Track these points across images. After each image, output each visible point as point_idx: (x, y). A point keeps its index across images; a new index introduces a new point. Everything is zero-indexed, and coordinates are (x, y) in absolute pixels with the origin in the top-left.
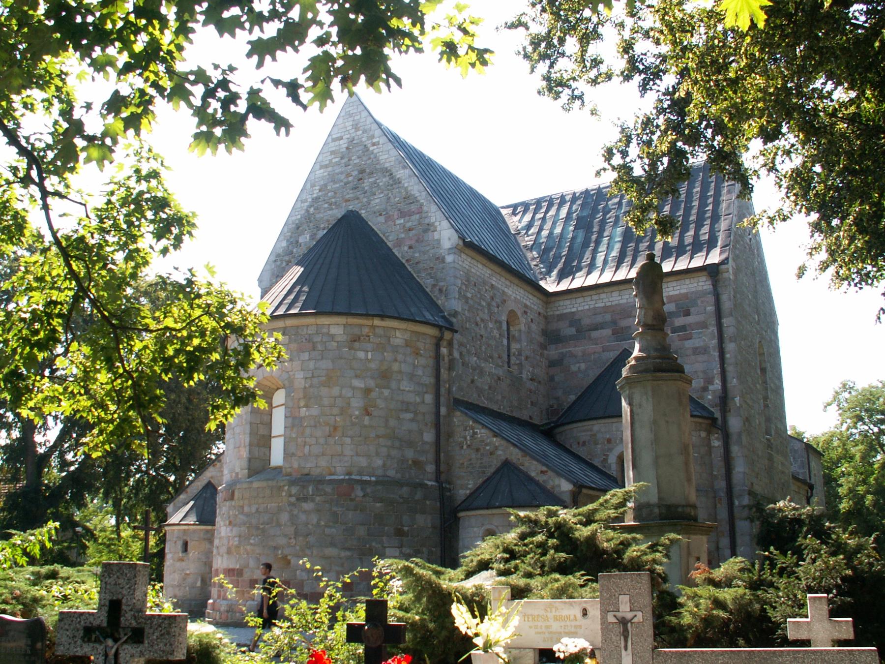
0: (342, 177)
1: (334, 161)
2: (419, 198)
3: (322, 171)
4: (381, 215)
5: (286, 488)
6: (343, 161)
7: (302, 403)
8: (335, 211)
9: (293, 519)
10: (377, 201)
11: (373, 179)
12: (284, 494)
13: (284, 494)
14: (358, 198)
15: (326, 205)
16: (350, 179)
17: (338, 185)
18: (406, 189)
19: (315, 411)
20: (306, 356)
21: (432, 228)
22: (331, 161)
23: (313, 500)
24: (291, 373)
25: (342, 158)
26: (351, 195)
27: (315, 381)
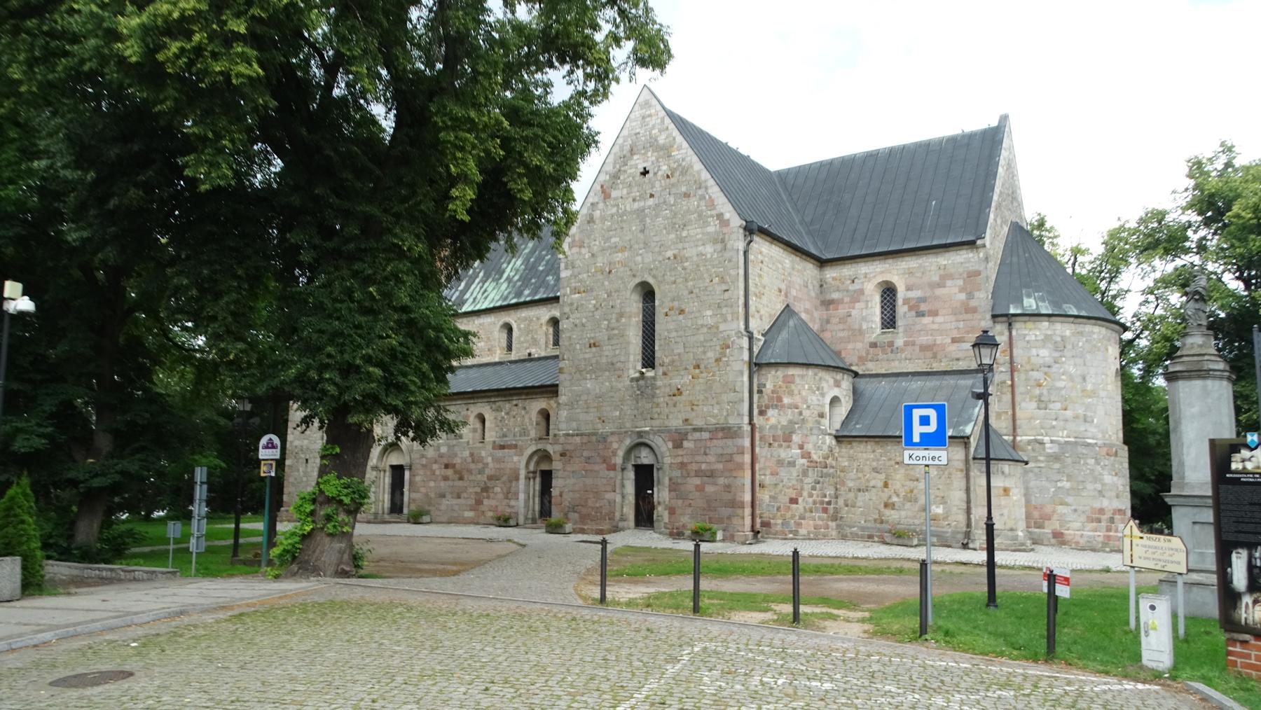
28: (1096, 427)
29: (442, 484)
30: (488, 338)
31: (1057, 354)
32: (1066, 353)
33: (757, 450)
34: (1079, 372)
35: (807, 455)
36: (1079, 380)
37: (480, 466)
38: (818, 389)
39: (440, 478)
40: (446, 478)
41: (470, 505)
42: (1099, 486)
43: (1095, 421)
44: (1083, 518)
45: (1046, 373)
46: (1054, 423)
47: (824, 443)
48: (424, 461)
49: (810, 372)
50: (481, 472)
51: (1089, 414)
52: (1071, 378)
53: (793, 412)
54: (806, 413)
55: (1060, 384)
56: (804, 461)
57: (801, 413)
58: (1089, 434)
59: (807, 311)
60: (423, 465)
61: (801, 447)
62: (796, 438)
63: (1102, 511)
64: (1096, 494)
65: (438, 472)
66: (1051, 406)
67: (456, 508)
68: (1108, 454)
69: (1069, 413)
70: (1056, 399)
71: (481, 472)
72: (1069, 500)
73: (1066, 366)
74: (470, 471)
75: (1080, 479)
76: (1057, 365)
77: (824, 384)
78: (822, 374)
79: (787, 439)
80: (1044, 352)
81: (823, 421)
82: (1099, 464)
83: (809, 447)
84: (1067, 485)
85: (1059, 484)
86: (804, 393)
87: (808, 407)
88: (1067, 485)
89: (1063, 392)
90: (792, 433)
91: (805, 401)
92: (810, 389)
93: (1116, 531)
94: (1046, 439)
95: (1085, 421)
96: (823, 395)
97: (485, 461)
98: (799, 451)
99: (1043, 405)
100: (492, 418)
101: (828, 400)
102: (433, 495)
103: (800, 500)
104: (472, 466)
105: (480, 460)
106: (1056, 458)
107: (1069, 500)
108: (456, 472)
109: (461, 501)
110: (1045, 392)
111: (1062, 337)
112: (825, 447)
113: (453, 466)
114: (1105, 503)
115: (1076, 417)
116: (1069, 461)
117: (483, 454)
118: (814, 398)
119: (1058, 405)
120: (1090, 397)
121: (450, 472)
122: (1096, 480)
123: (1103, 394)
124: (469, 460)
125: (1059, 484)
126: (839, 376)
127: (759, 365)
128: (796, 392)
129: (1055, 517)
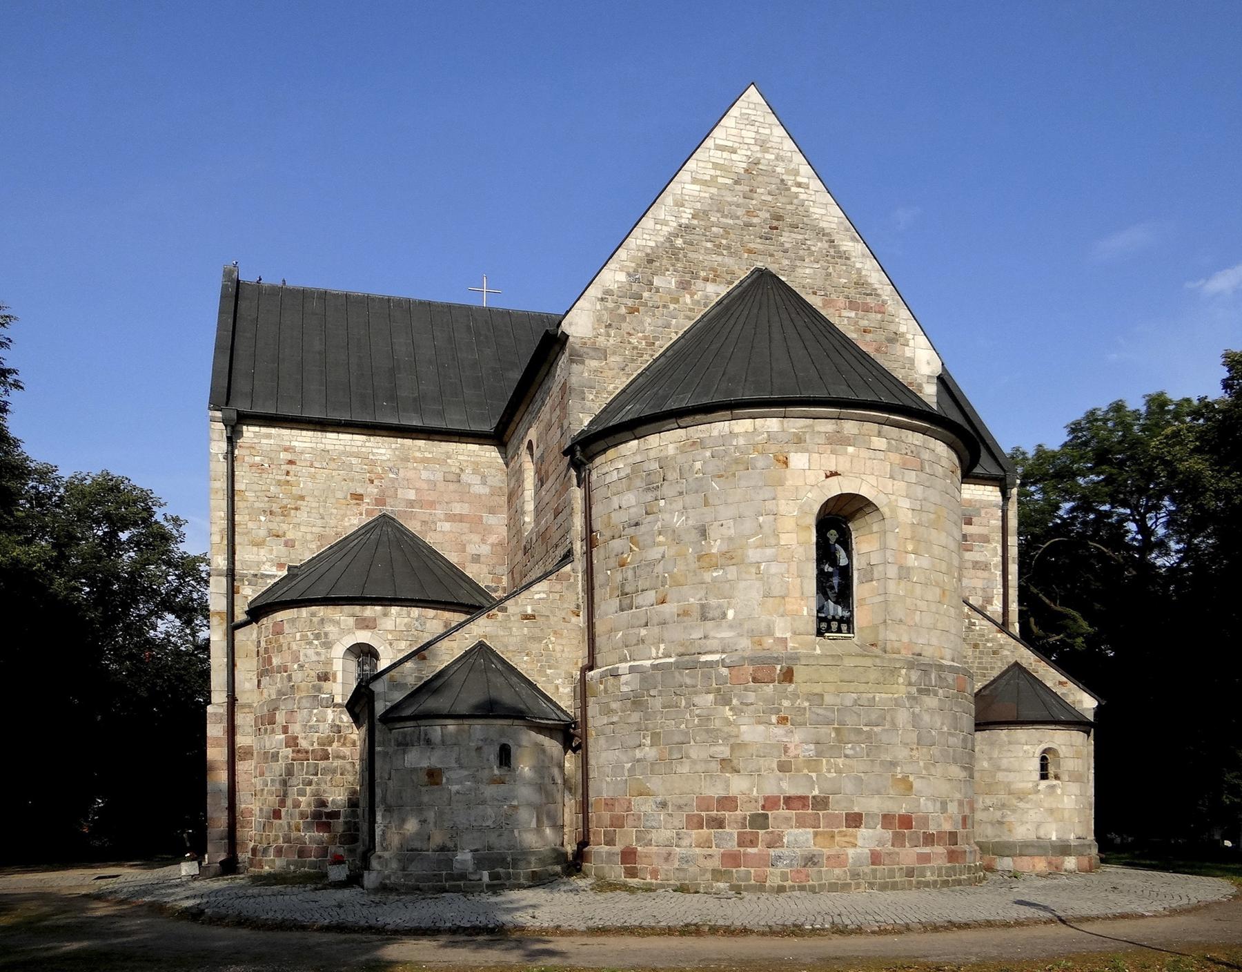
0: (740, 212)
1: (720, 180)
2: (879, 292)
3: (697, 187)
4: (815, 293)
5: (903, 671)
6: (738, 187)
7: (910, 548)
8: (730, 261)
9: (915, 719)
10: (807, 271)
11: (800, 237)
12: (901, 680)
13: (901, 680)
14: (771, 255)
15: (709, 245)
16: (755, 220)
17: (731, 222)
18: (859, 271)
19: (925, 562)
20: (912, 476)
21: (902, 340)
22: (714, 178)
23: (936, 695)
24: (893, 498)
25: (737, 182)
26: (760, 247)
27: (925, 517)
28: (731, 627)
31: (649, 497)
32: (667, 490)
33: (242, 740)
34: (690, 522)
35: (292, 742)
36: (694, 535)
38: (317, 637)
42: (723, 751)
43: (731, 614)
44: (679, 819)
45: (632, 539)
46: (643, 632)
47: (321, 719)
49: (305, 612)
51: (713, 602)
52: (676, 538)
53: (282, 677)
54: (298, 677)
55: (655, 553)
56: (289, 751)
57: (290, 678)
58: (712, 644)
59: (450, 518)
61: (285, 730)
62: (280, 718)
63: (728, 802)
64: (714, 766)
66: (639, 600)
68: (755, 680)
69: (670, 608)
70: (647, 585)
72: (655, 783)
73: (667, 516)
75: (677, 738)
76: (650, 518)
77: (330, 628)
78: (321, 611)
79: (272, 722)
80: (630, 499)
81: (326, 685)
82: (727, 702)
83: (296, 729)
84: (649, 752)
85: (638, 754)
86: (294, 647)
87: (301, 667)
88: (649, 752)
89: (659, 569)
90: (276, 709)
91: (296, 659)
92: (304, 637)
93: (807, 840)
94: (623, 667)
95: (704, 618)
96: (328, 645)
98: (283, 736)
99: (626, 602)
101: (339, 650)
103: (283, 811)
106: (636, 702)
107: (655, 783)
110: (630, 574)
111: (659, 460)
112: (325, 730)
114: (738, 785)
115: (685, 613)
116: (657, 703)
118: (311, 652)
119: (651, 596)
120: (716, 567)
122: (713, 736)
123: (753, 555)
125: (638, 754)
126: (370, 611)
127: (257, 612)
128: (285, 647)
129: (630, 821)
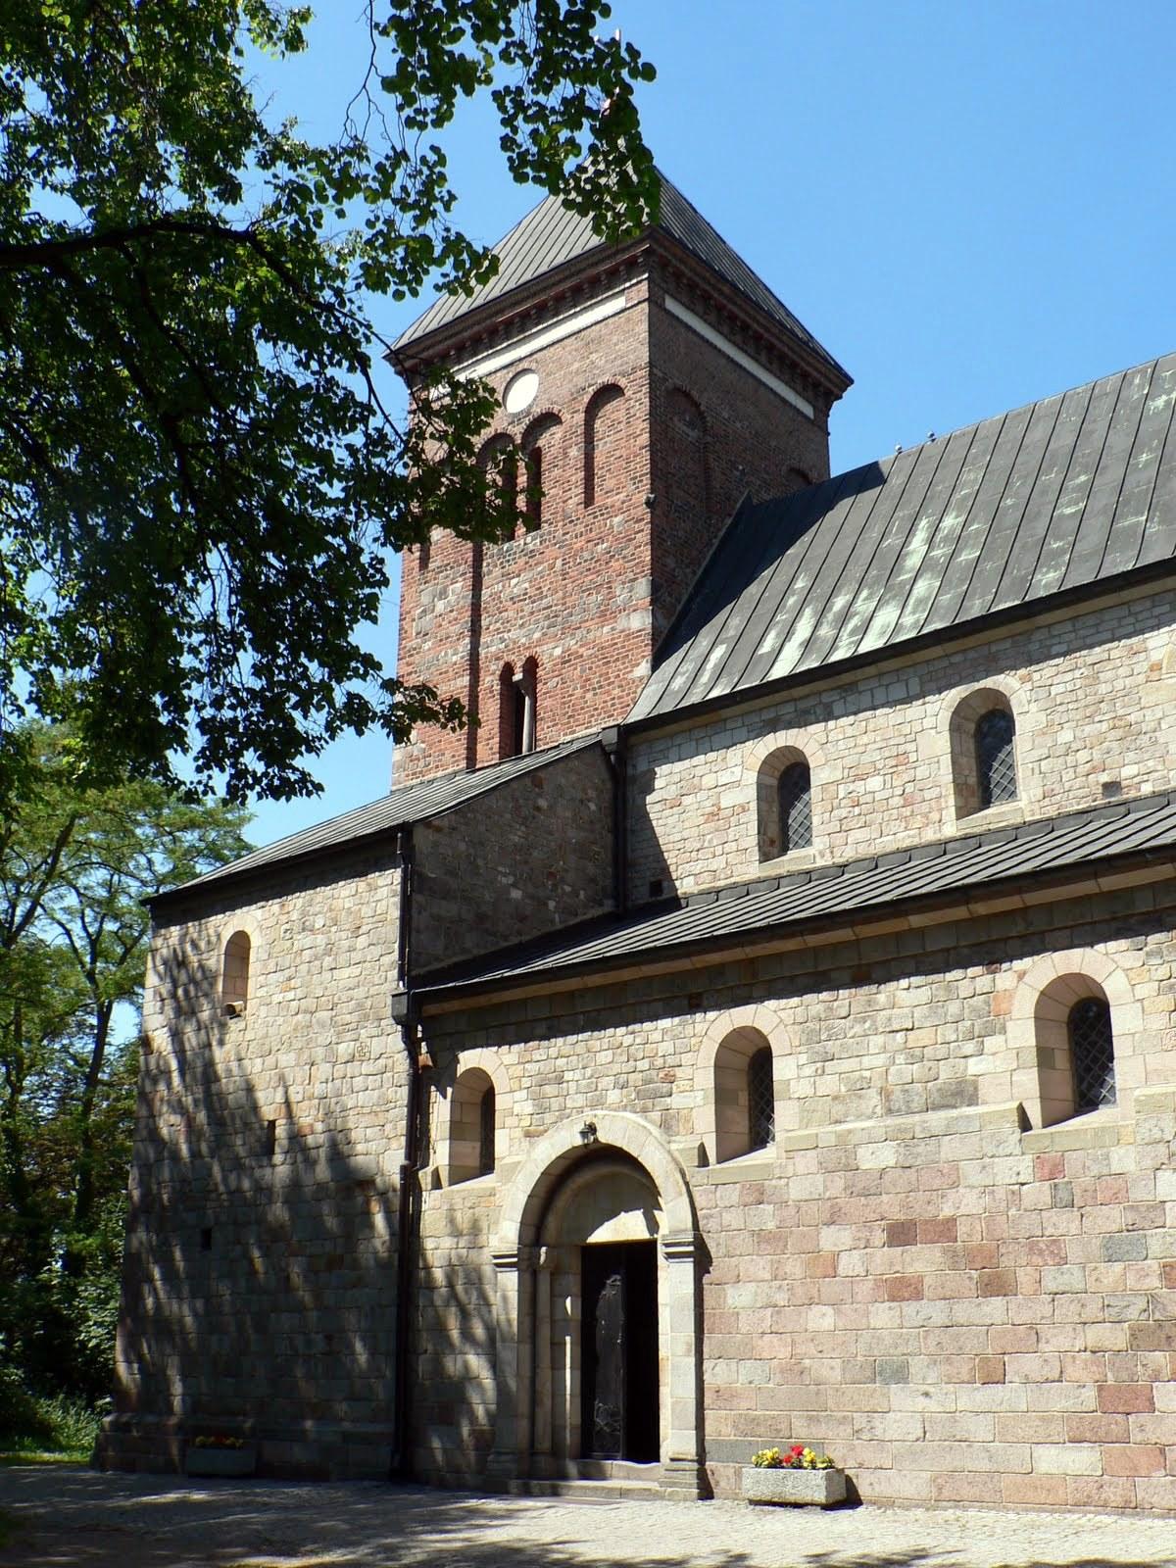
29: (883, 1315)
30: (901, 760)
37: (1112, 1218)
39: (865, 1289)
40: (904, 1290)
41: (1067, 1415)
48: (767, 1217)
50: (1113, 1251)
60: (761, 1237)
65: (850, 1264)
67: (980, 1429)
71: (1113, 1251)
74: (1054, 1251)
97: (1139, 1194)
100: (1146, 990)
102: (830, 1370)
104: (1063, 1223)
105: (1114, 1189)
108: (955, 1260)
109: (1011, 1395)
113: (945, 1230)
117: (1124, 1159)
121: (923, 1260)
124: (1038, 1193)
